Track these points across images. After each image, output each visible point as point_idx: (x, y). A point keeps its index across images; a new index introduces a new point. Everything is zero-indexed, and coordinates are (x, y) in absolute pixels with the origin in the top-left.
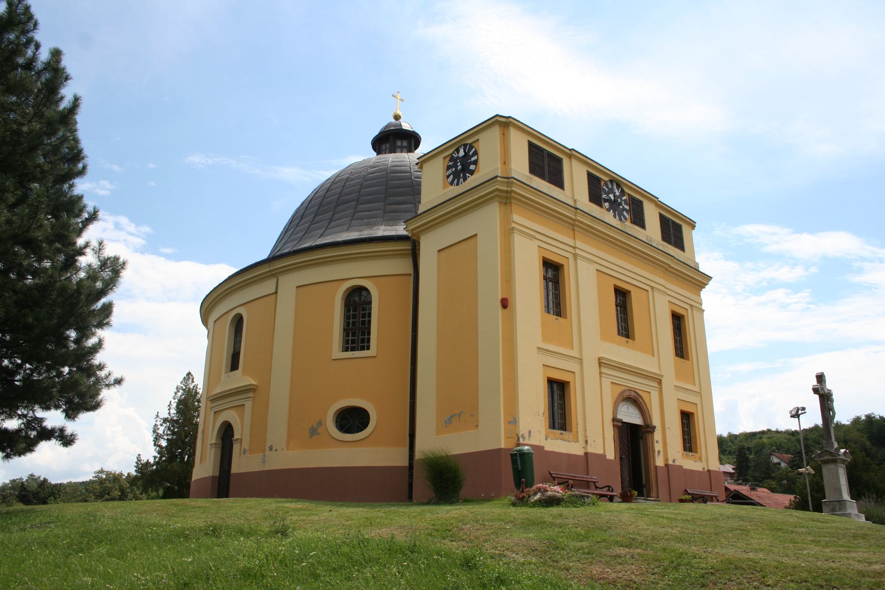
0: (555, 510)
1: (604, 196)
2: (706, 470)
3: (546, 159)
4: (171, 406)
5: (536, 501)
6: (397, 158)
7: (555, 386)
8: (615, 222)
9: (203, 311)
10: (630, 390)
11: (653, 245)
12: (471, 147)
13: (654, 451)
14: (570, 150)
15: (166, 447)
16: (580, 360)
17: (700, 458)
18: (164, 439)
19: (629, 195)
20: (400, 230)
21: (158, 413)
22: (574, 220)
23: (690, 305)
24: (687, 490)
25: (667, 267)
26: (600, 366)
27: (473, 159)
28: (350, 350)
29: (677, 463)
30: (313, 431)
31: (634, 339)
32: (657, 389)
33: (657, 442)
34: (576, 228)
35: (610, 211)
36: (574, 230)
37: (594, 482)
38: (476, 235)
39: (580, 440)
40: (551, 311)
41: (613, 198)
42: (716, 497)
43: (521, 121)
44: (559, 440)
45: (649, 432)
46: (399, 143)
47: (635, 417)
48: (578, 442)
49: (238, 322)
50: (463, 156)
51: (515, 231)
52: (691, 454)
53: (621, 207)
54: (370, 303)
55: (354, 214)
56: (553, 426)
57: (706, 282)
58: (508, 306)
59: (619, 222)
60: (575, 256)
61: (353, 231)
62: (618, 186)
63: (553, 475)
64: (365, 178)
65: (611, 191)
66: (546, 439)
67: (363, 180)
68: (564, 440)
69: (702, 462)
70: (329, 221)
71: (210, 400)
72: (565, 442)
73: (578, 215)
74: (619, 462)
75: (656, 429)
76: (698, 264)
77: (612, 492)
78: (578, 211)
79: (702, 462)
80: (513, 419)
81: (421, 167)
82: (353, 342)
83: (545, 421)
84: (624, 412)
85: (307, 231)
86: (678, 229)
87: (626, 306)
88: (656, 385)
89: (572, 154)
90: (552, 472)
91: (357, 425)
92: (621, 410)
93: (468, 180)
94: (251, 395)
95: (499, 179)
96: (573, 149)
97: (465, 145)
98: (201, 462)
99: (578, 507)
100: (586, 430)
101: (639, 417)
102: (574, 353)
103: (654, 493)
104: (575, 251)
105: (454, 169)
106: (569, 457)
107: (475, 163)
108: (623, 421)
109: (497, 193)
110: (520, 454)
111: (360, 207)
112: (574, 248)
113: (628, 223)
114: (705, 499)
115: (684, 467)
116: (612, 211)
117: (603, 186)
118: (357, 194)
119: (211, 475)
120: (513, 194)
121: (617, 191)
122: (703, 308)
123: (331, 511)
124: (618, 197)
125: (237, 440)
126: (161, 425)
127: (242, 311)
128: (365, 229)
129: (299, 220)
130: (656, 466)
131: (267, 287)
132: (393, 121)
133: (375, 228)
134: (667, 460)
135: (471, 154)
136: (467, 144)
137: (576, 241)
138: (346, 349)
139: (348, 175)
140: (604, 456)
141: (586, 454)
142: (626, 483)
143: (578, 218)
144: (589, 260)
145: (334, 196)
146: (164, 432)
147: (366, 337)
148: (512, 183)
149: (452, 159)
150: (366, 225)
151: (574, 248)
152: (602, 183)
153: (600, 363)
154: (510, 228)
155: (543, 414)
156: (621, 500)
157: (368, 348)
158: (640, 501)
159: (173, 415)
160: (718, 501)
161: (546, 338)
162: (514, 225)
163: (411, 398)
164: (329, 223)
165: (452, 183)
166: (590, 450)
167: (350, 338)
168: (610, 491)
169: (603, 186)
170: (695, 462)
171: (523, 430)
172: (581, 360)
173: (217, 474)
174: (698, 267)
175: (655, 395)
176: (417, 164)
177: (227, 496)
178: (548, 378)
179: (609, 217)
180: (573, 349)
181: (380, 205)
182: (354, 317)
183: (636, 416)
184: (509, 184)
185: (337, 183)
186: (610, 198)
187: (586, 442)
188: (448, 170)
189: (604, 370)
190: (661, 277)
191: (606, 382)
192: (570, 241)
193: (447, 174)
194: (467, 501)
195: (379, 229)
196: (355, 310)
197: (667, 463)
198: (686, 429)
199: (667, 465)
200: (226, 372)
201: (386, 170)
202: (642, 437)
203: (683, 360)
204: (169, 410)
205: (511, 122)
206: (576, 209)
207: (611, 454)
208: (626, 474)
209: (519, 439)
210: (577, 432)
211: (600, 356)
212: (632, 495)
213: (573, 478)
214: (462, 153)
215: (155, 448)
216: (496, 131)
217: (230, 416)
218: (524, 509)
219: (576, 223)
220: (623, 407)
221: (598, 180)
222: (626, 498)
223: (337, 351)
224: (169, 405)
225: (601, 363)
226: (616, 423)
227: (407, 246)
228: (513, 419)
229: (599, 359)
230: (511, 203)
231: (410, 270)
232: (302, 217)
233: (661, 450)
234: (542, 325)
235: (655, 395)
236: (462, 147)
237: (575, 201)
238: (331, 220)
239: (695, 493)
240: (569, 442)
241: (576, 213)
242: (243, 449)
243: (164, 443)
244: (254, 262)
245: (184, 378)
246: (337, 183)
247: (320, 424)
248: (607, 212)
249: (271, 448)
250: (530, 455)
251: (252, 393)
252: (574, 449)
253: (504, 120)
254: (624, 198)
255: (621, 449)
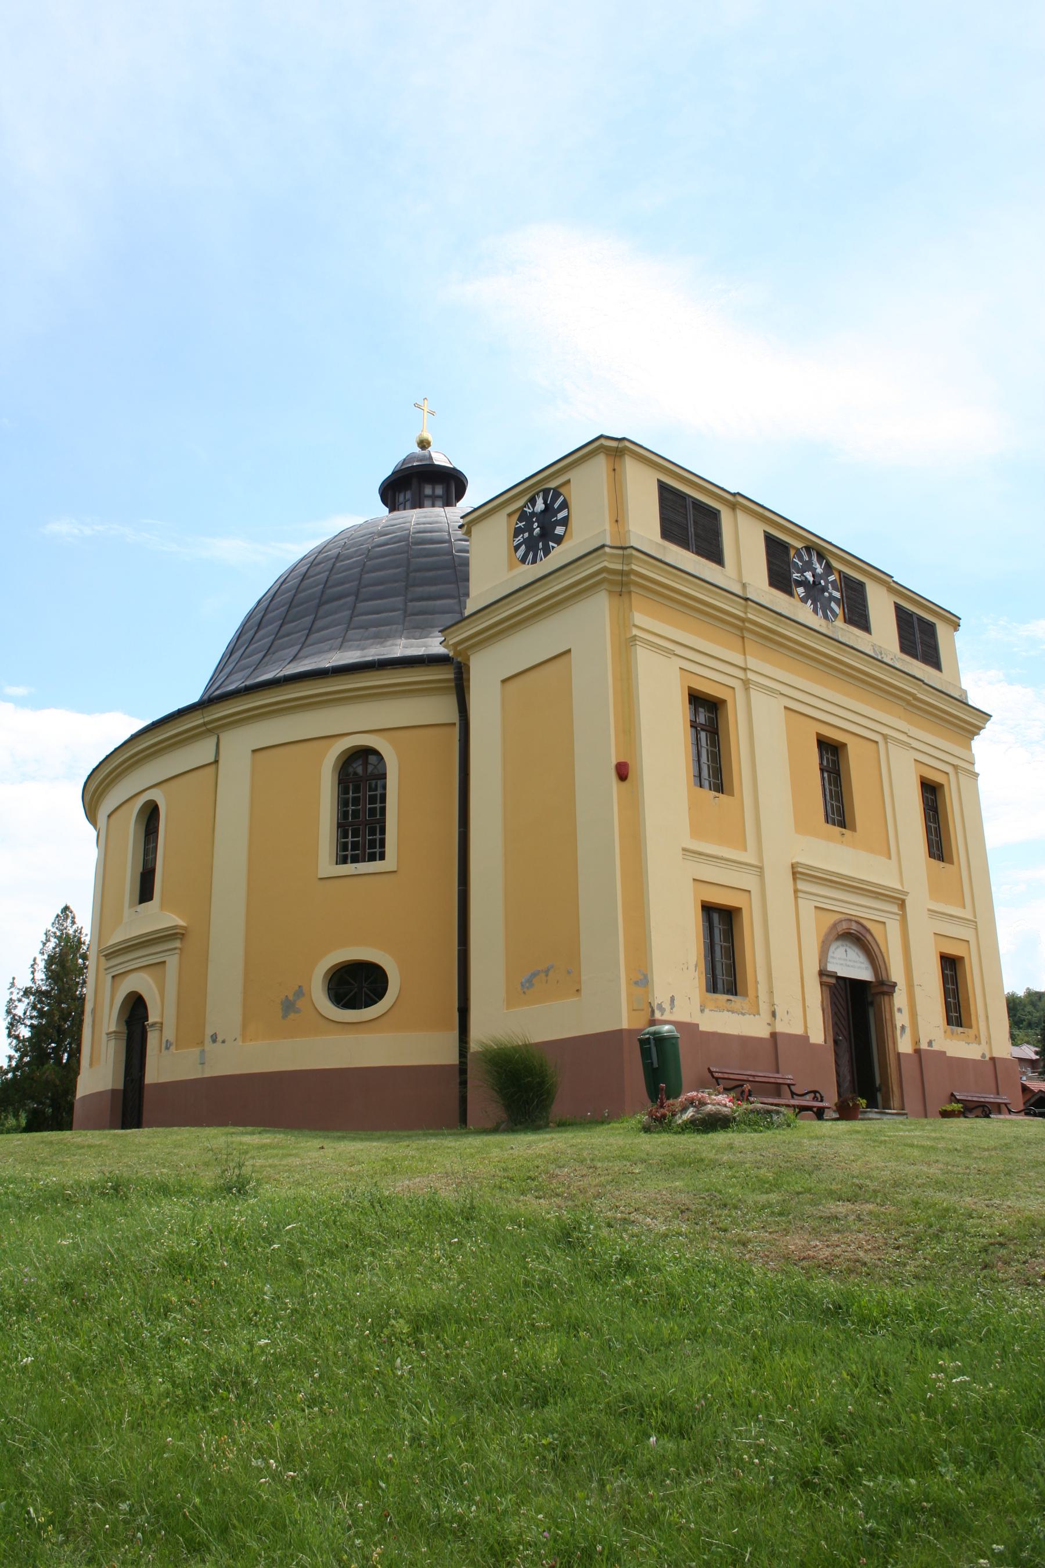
0: (720, 1138)
1: (796, 576)
2: (987, 1058)
3: (691, 511)
4: (35, 966)
5: (685, 1123)
6: (425, 517)
7: (716, 917)
8: (816, 621)
9: (87, 798)
11: (885, 660)
12: (557, 494)
13: (894, 1027)
14: (734, 495)
15: (30, 1039)
16: (760, 870)
17: (976, 1037)
18: (26, 1026)
19: (840, 572)
20: (434, 645)
21: (14, 978)
22: (743, 620)
23: (953, 765)
24: (955, 1093)
25: (911, 699)
26: (795, 879)
27: (560, 516)
28: (349, 860)
29: (936, 1047)
30: (289, 1007)
31: (853, 829)
32: (898, 918)
33: (900, 1010)
34: (746, 634)
35: (806, 603)
36: (743, 638)
37: (789, 1085)
38: (569, 651)
39: (761, 1011)
40: (706, 783)
41: (811, 579)
42: (1006, 1104)
43: (645, 446)
44: (725, 1012)
45: (884, 993)
46: (428, 490)
47: (859, 968)
48: (759, 1014)
49: (151, 815)
50: (542, 512)
51: (638, 643)
52: (960, 1029)
53: (826, 594)
54: (383, 776)
55: (351, 618)
56: (713, 987)
57: (981, 725)
58: (629, 778)
59: (823, 622)
60: (746, 683)
61: (350, 648)
62: (821, 557)
63: (716, 1075)
64: (368, 554)
65: (808, 566)
66: (702, 1011)
67: (366, 557)
68: (733, 1012)
69: (979, 1043)
70: (306, 632)
71: (105, 956)
72: (735, 1015)
73: (749, 610)
74: (833, 1048)
75: (896, 988)
76: (965, 692)
77: (822, 1101)
78: (750, 603)
79: (979, 1043)
80: (642, 977)
81: (468, 533)
82: (355, 846)
83: (699, 978)
84: (839, 959)
85: (269, 651)
86: (929, 630)
87: (839, 770)
88: (895, 909)
89: (737, 502)
90: (713, 1069)
91: (366, 994)
92: (835, 956)
93: (553, 553)
94: (177, 944)
95: (607, 550)
96: (738, 493)
97: (546, 492)
98: (91, 1065)
99: (761, 1132)
100: (772, 992)
101: (866, 968)
102: (749, 857)
103: (895, 1101)
104: (746, 674)
105: (526, 535)
106: (744, 1041)
107: (565, 522)
108: (839, 975)
109: (604, 575)
110: (654, 1039)
111: (362, 606)
112: (745, 669)
113: (839, 623)
114: (986, 1109)
115: (948, 1054)
116: (810, 602)
117: (794, 557)
118: (356, 583)
119: (110, 1087)
120: (633, 577)
121: (818, 566)
122: (977, 771)
123: (322, 1148)
124: (821, 576)
125: (153, 1025)
126: (20, 1000)
127: (156, 795)
128: (372, 644)
129: (252, 632)
130: (899, 1054)
131: (201, 752)
132: (417, 450)
133: (389, 643)
134: (917, 1042)
135: (556, 506)
136: (549, 490)
137: (748, 657)
138: (343, 860)
139: (339, 550)
140: (806, 1038)
141: (774, 1035)
142: (846, 1084)
143: (750, 616)
145: (316, 586)
146: (25, 1013)
147: (378, 836)
148: (631, 556)
149: (523, 516)
150: (372, 638)
151: (745, 669)
152: (792, 552)
153: (794, 874)
154: (628, 636)
155: (696, 966)
156: (837, 1116)
157: (382, 857)
158: (871, 1116)
159: (41, 983)
160: (1010, 1112)
161: (697, 830)
162: (635, 632)
163: (459, 945)
164: (308, 635)
165: (523, 560)
166: (780, 1028)
167: (350, 839)
168: (817, 1100)
169: (794, 557)
170: (969, 1044)
171: (660, 995)
172: (761, 868)
173: (120, 1086)
174: (966, 697)
175: (893, 928)
176: (461, 527)
177: (139, 1125)
178: (702, 902)
179: (805, 613)
180: (746, 850)
181: (398, 600)
182: (356, 801)
183: (863, 966)
184: (626, 559)
185: (319, 564)
186: (806, 578)
187: (774, 1014)
188: (516, 536)
189: (802, 885)
190: (900, 718)
191: (807, 907)
192: (737, 658)
193: (515, 543)
194: (563, 1125)
195: (396, 645)
196: (357, 789)
197: (917, 1047)
198: (950, 986)
199: (918, 1051)
200: (131, 906)
201: (405, 538)
202: (872, 1004)
203: (942, 864)
204: (33, 973)
205: (626, 448)
206: (747, 599)
207: (818, 1035)
208: (845, 1070)
209: (653, 1012)
210: (757, 997)
211: (794, 861)
212: (856, 1106)
213: (751, 1079)
214: (540, 506)
215: (10, 1040)
216: (600, 464)
217: (141, 983)
218: (665, 1138)
219: (747, 625)
220: (838, 950)
221: (785, 547)
222: (846, 1112)
223: (326, 864)
224: (32, 966)
225: (796, 873)
226: (825, 979)
227: (446, 674)
228: (642, 977)
229: (793, 866)
230: (630, 592)
231: (454, 717)
232: (259, 625)
233: (907, 1024)
234: (690, 809)
235: (893, 928)
236: (541, 494)
237: (744, 586)
238: (310, 630)
239: (970, 1098)
240: (743, 1014)
241: (746, 607)
242: (164, 1041)
243: (25, 1032)
244: (176, 709)
245: (58, 916)
246: (319, 564)
247: (300, 992)
248: (800, 604)
249: (214, 1039)
250: (674, 1041)
251: (178, 941)
252: (756, 1027)
253: (614, 444)
254: (831, 578)
255: (835, 1025)
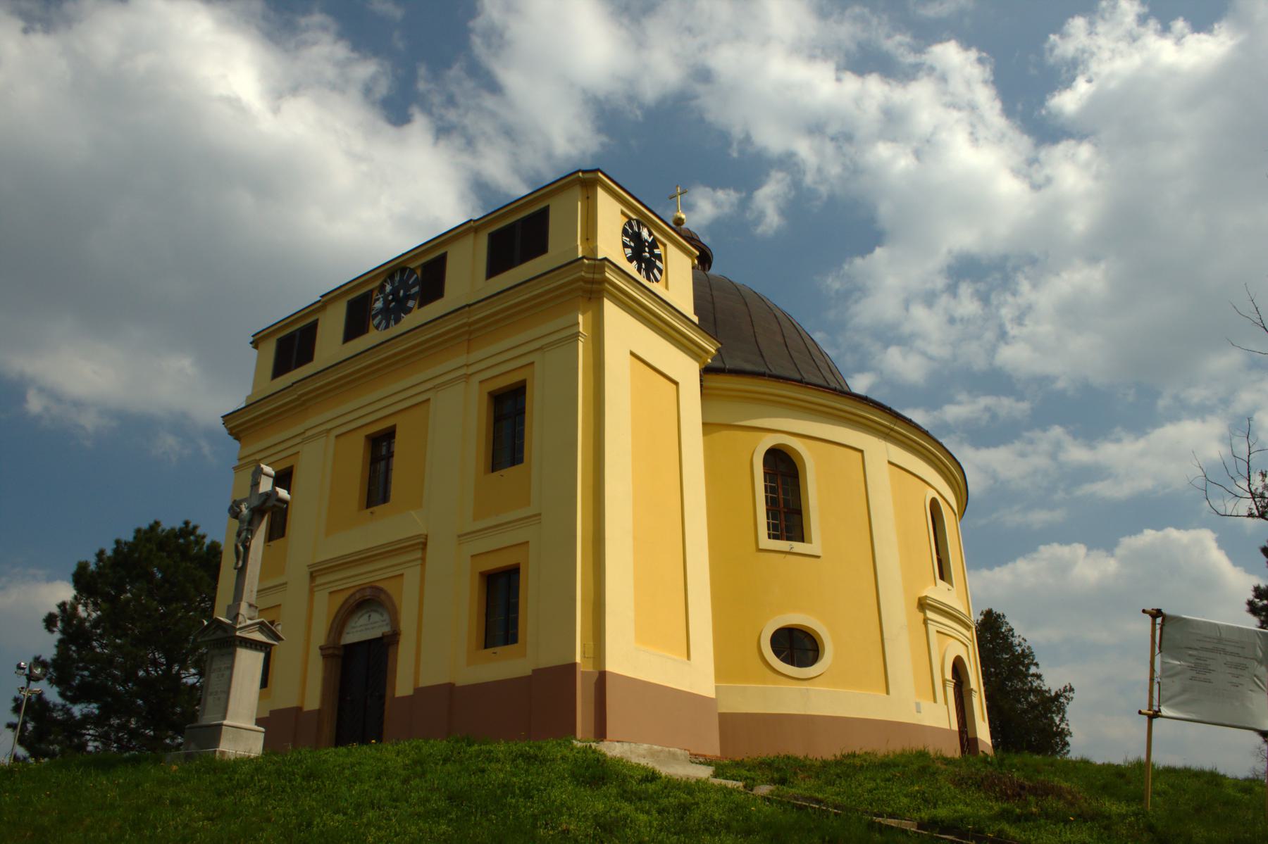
10: (362, 589)
22: (301, 396)
25: (467, 328)
78: (295, 385)
96: (322, 297)
143: (299, 393)
144: (320, 433)
183: (385, 623)
189: (319, 581)
219: (303, 399)
